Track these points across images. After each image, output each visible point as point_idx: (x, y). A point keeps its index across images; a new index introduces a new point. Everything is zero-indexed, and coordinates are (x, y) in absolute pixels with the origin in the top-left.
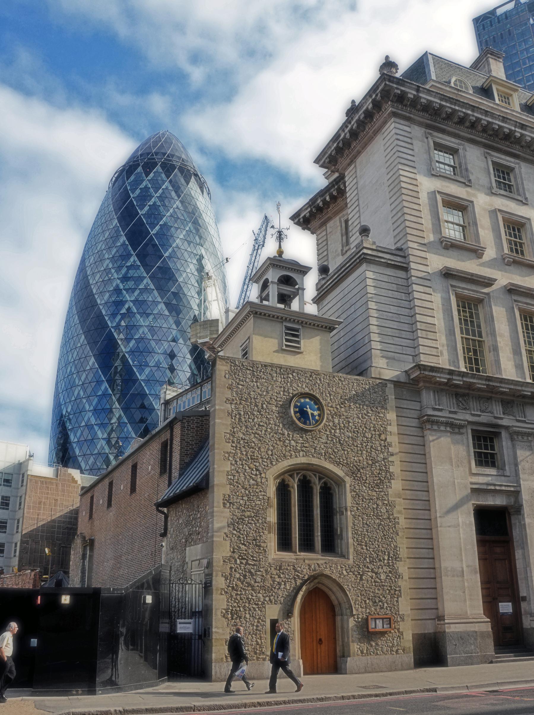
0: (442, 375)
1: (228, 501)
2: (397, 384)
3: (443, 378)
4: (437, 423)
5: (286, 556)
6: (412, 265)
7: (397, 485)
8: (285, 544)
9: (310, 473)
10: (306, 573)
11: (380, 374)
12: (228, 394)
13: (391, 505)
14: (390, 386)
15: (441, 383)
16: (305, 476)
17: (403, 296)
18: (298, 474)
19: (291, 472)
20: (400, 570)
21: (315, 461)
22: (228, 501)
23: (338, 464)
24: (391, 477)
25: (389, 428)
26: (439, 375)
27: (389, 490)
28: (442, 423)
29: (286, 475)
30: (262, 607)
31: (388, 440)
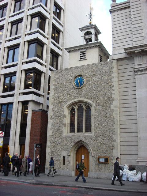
0: (137, 49)
1: (52, 118)
2: (118, 60)
3: (138, 50)
4: (139, 71)
5: (72, 134)
6: (131, 4)
7: (116, 103)
8: (72, 130)
9: (81, 104)
10: (76, 140)
11: (113, 58)
12: (54, 83)
13: (113, 111)
14: (116, 61)
15: (138, 53)
16: (81, 105)
17: (129, 19)
18: (77, 105)
19: (74, 104)
20: (115, 138)
21: (81, 99)
22: (52, 118)
23: (90, 98)
24: (112, 100)
25: (113, 80)
26: (136, 49)
27: (112, 105)
28: (142, 70)
29: (73, 106)
30: (60, 152)
31: (112, 85)
